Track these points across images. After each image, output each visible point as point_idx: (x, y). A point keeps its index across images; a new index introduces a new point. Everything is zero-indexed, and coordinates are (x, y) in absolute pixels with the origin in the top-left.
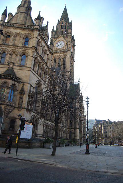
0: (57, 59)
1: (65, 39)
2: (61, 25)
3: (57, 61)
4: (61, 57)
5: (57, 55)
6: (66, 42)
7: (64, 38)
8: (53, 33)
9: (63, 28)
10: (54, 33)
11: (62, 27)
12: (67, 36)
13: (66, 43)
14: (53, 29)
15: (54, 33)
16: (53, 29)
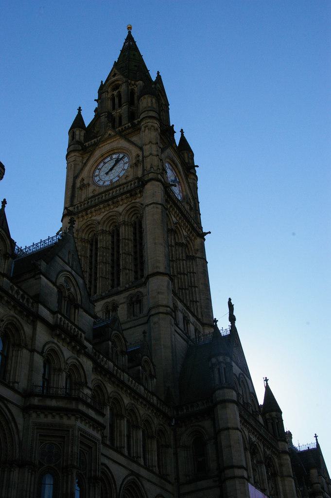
2: (109, 95)
4: (121, 219)
5: (99, 218)
6: (135, 151)
7: (124, 135)
8: (77, 132)
11: (116, 102)
13: (134, 154)
14: (79, 121)
15: (80, 134)
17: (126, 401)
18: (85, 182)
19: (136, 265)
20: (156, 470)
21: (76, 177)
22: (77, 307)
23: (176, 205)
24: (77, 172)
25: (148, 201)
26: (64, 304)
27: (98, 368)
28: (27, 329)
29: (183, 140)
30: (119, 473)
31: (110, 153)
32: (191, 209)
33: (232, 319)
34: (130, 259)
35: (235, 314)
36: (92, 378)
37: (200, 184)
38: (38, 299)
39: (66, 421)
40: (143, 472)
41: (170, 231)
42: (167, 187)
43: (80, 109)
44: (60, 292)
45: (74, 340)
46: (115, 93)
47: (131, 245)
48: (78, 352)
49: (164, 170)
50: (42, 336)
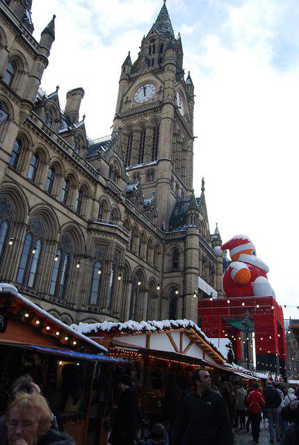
0: (137, 131)
1: (157, 77)
3: (137, 136)
4: (147, 124)
5: (135, 122)
7: (155, 73)
8: (127, 68)
9: (154, 53)
11: (152, 50)
12: (161, 70)
13: (159, 86)
14: (129, 58)
15: (128, 69)
16: (129, 58)
17: (141, 228)
19: (153, 153)
20: (152, 265)
22: (119, 177)
23: (180, 119)
25: (164, 116)
26: (112, 175)
27: (127, 211)
28: (92, 188)
29: (189, 77)
30: (133, 265)
32: (188, 122)
33: (203, 189)
34: (150, 149)
35: (205, 187)
36: (123, 216)
37: (195, 106)
38: (99, 172)
39: (109, 238)
40: (146, 265)
41: (175, 134)
42: (176, 108)
43: (129, 53)
44: (111, 169)
45: (116, 196)
46: (152, 44)
47: (152, 140)
48: (118, 202)
49: (176, 97)
50: (100, 192)
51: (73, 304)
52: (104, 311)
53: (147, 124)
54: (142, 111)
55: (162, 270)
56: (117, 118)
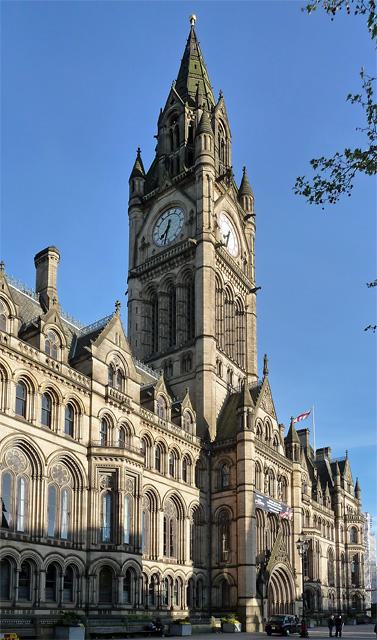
0: (162, 294)
4: (176, 281)
10: (142, 184)
15: (140, 184)
18: (146, 242)
21: (137, 236)
24: (138, 230)
31: (169, 207)
47: (185, 307)
51: (81, 544)
52: (119, 548)
53: (176, 281)
54: (164, 261)
55: (210, 490)
56: (132, 276)
